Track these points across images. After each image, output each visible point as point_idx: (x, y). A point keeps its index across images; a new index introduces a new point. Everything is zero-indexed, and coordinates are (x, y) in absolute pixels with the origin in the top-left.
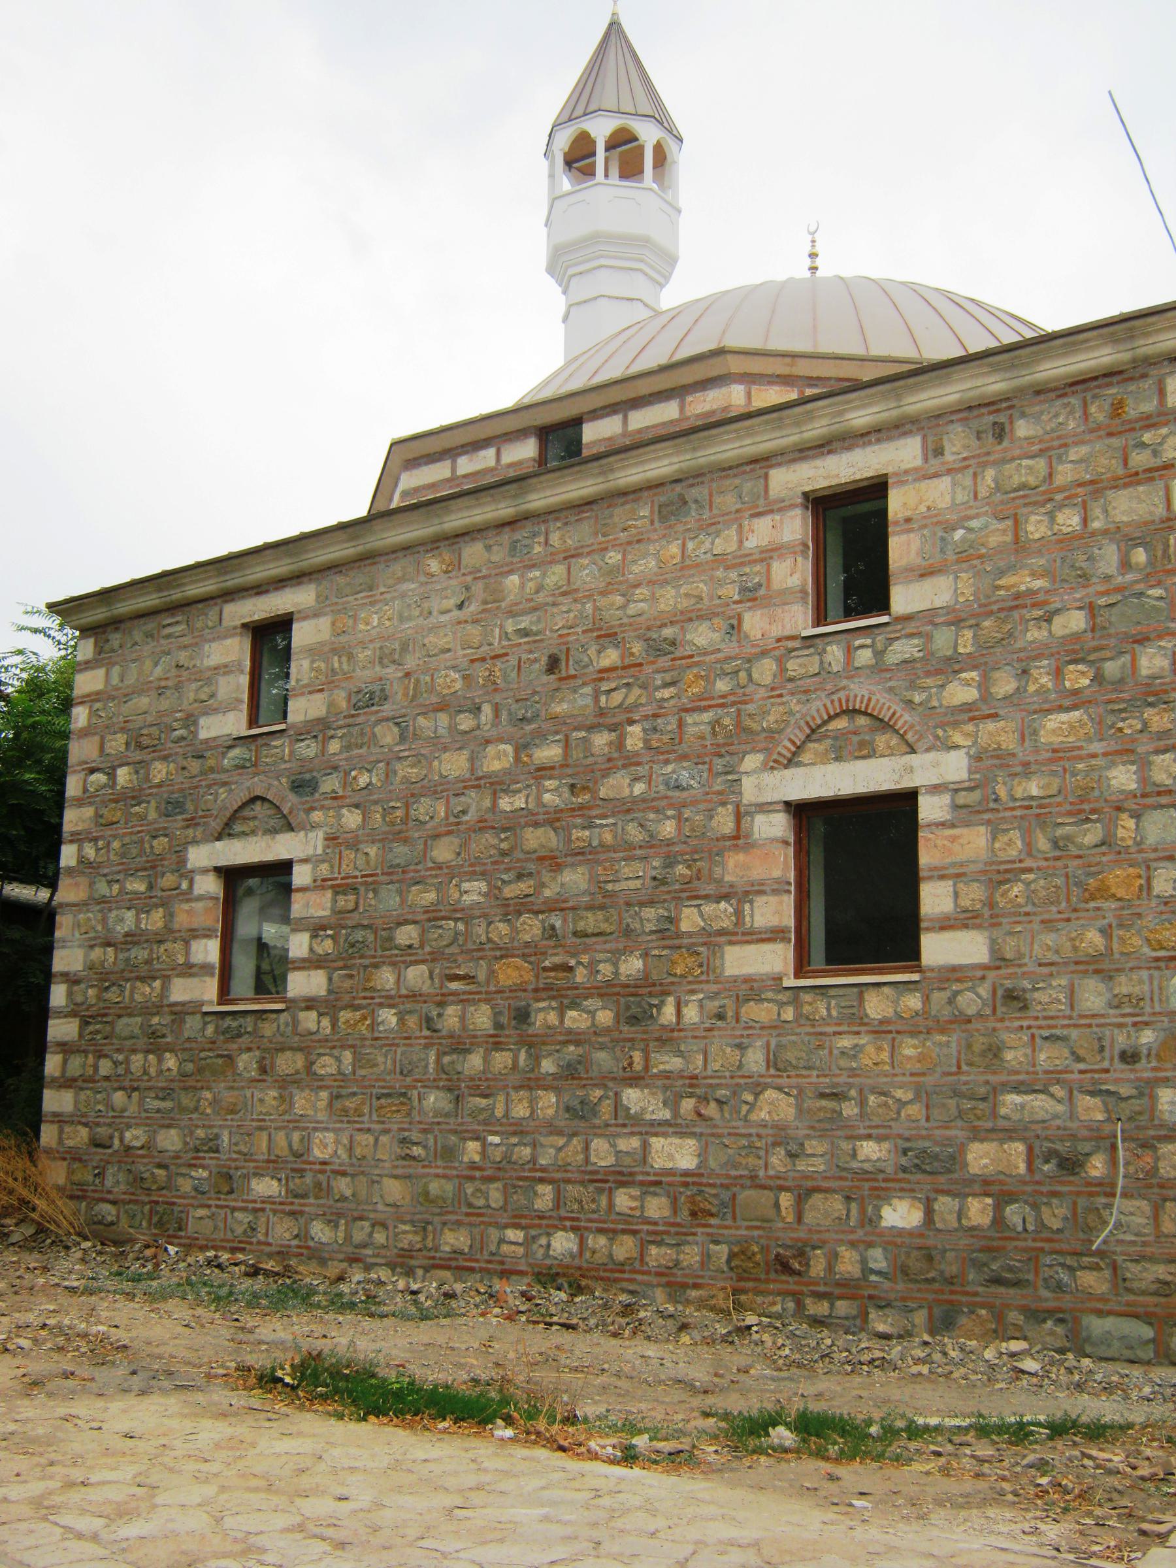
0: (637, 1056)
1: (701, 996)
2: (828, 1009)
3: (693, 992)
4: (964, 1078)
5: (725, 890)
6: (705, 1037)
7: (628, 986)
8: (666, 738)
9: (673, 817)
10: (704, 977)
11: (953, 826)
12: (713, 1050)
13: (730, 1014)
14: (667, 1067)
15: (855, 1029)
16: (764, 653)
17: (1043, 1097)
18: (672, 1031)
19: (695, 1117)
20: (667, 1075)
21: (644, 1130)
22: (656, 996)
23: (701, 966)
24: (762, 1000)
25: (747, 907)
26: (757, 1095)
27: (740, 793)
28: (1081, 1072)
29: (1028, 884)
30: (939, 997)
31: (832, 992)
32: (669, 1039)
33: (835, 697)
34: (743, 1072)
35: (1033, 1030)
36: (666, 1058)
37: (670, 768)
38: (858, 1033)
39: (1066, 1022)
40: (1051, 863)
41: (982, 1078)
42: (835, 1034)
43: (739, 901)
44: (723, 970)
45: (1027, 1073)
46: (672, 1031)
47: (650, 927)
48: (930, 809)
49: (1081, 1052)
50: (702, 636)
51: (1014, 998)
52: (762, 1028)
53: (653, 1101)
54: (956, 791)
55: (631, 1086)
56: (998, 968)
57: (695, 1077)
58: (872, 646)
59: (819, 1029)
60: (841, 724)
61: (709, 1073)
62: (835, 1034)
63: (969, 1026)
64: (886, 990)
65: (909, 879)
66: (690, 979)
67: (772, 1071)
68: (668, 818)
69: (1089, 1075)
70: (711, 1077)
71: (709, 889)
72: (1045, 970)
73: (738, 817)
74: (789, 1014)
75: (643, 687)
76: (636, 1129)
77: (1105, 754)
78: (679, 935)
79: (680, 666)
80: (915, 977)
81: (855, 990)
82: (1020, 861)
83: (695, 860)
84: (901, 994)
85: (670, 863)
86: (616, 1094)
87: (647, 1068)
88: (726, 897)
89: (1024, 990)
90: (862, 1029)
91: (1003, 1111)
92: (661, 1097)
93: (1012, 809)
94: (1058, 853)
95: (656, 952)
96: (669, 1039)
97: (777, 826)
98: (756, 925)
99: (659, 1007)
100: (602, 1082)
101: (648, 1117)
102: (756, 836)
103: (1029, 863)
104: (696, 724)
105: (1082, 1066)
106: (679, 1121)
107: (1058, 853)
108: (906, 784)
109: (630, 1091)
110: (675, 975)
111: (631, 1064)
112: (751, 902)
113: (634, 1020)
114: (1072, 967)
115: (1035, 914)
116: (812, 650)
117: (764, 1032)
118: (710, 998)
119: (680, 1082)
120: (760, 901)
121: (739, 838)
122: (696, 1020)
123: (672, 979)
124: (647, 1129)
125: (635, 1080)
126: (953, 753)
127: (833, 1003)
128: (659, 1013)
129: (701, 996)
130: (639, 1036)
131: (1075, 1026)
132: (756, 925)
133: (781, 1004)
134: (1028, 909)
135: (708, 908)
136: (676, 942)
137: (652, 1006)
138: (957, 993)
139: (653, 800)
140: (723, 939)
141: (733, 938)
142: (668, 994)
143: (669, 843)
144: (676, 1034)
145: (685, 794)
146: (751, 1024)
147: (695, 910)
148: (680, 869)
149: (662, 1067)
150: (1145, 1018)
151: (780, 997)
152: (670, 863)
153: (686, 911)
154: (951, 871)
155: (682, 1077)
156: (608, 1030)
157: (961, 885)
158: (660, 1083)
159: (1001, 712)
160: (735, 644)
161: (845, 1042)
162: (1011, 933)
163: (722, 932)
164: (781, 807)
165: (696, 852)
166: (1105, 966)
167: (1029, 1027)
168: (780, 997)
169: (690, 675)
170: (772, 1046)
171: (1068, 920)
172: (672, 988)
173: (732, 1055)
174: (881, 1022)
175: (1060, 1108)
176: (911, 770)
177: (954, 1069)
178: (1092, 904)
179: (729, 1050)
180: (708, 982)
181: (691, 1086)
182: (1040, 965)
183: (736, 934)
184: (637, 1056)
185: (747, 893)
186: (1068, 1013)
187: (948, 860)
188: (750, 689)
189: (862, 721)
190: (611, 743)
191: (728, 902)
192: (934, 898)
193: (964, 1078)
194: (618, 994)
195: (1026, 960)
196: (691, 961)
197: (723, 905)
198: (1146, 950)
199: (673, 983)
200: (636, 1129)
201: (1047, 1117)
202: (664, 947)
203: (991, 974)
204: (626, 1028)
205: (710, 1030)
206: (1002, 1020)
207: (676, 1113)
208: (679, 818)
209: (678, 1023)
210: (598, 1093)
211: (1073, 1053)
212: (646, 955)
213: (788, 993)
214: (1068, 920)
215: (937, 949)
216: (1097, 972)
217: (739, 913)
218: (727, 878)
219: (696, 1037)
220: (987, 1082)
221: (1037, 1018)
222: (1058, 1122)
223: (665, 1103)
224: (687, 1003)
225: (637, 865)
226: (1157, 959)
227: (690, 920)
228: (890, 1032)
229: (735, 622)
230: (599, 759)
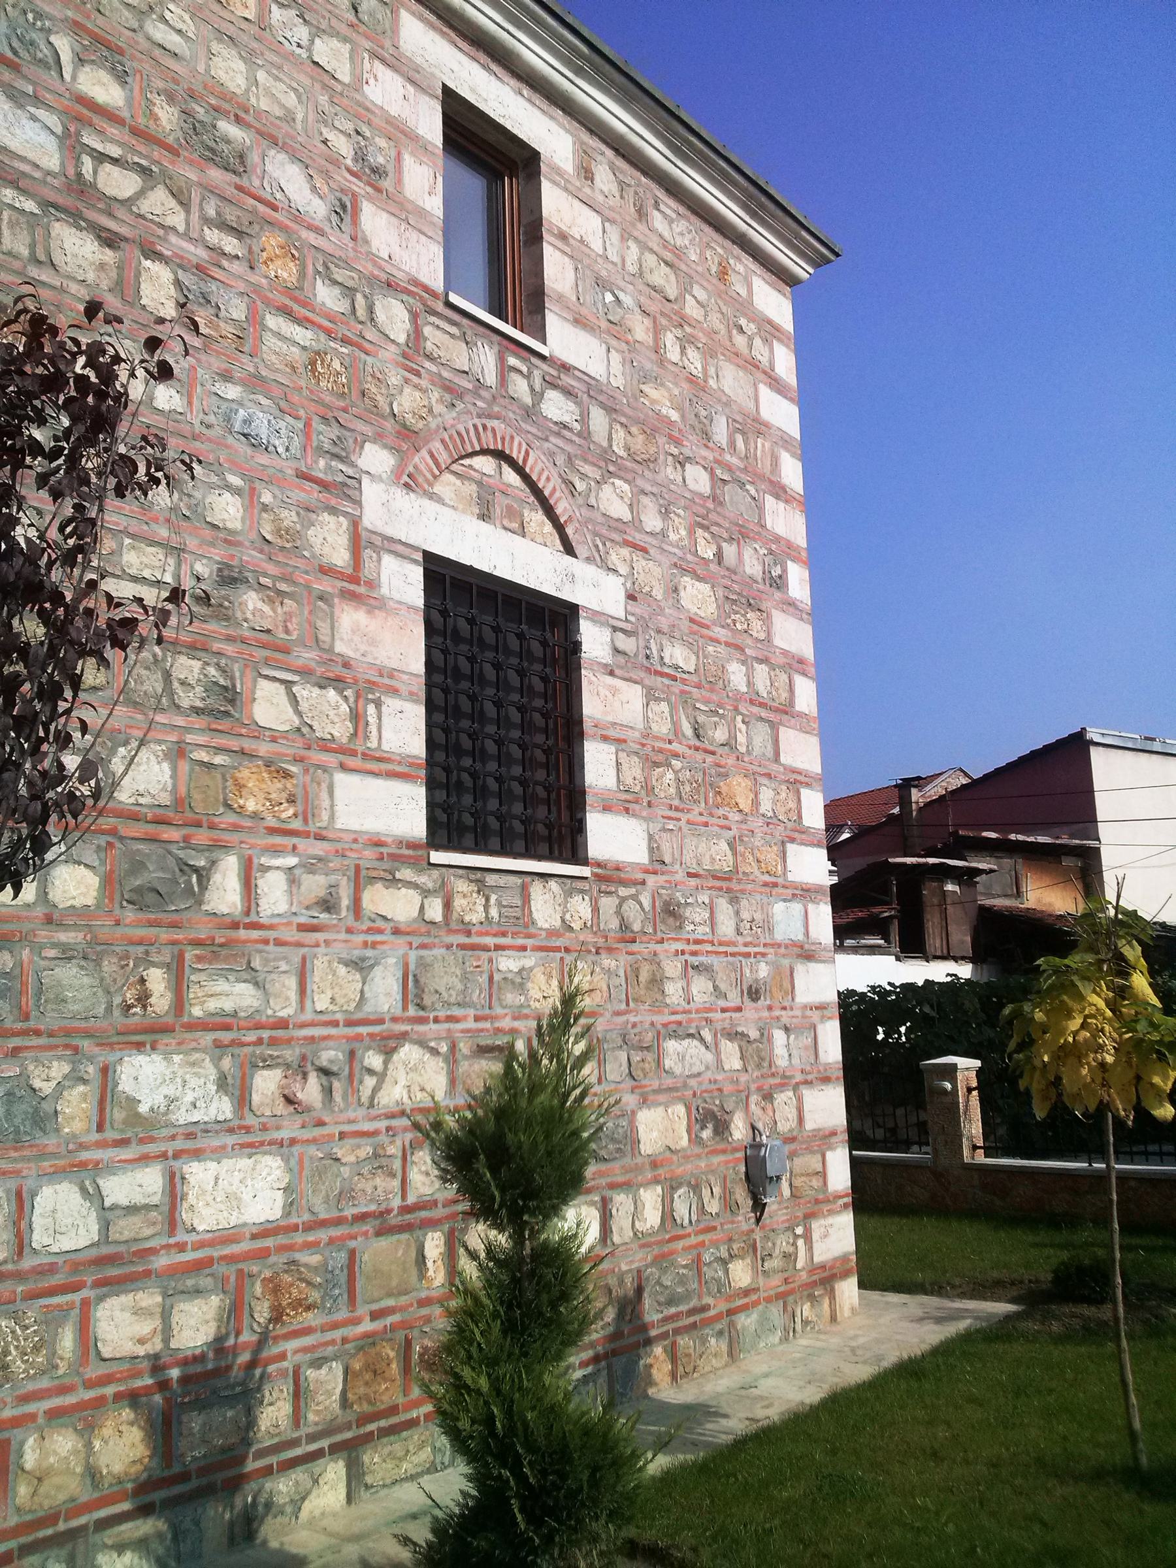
0: (157, 980)
1: (292, 861)
2: (486, 907)
3: (276, 851)
4: (632, 1018)
5: (339, 670)
6: (299, 945)
7: (134, 817)
8: (228, 329)
9: (237, 491)
10: (296, 825)
11: (611, 673)
12: (320, 965)
13: (345, 902)
14: (228, 1005)
15: (520, 941)
16: (390, 286)
17: (696, 1042)
18: (235, 926)
19: (281, 1108)
20: (222, 1023)
21: (170, 1147)
22: (198, 849)
23: (291, 801)
24: (393, 882)
25: (371, 709)
26: (388, 1053)
27: (358, 503)
28: (724, 1010)
29: (676, 772)
30: (608, 904)
31: (491, 879)
32: (233, 944)
33: (490, 423)
34: (368, 1009)
35: (687, 957)
36: (222, 986)
37: (232, 392)
38: (523, 948)
39: (709, 948)
40: (691, 752)
41: (648, 1018)
42: (498, 948)
43: (358, 696)
44: (332, 817)
45: (685, 1012)
46: (235, 926)
47: (187, 699)
48: (593, 642)
49: (723, 986)
50: (288, 179)
51: (671, 912)
52: (396, 932)
53: (193, 1082)
54: (615, 629)
55: (139, 1046)
56: (655, 873)
57: (283, 1024)
58: (528, 377)
59: (475, 940)
60: (486, 464)
61: (308, 1016)
62: (498, 948)
63: (634, 947)
64: (553, 884)
65: (568, 730)
66: (271, 822)
67: (412, 1011)
68: (228, 487)
69: (728, 1014)
70: (312, 1024)
71: (306, 656)
72: (693, 882)
73: (358, 541)
74: (435, 911)
75: (181, 197)
76: (151, 1148)
77: (727, 644)
78: (258, 732)
79: (254, 212)
80: (585, 871)
81: (518, 880)
82: (670, 742)
83: (279, 593)
84: (569, 894)
85: (230, 578)
86: (105, 1070)
87: (179, 1005)
88: (338, 683)
89: (679, 905)
90: (529, 942)
91: (668, 1063)
92: (213, 1074)
93: (662, 674)
94: (698, 744)
95: (203, 756)
96: (233, 944)
97: (406, 585)
98: (385, 747)
99: (203, 875)
100: (67, 1040)
101: (182, 1116)
102: (384, 591)
103: (675, 746)
104: (278, 335)
105: (722, 1003)
106: (250, 1120)
107: (698, 744)
108: (566, 595)
109: (141, 1059)
110: (240, 811)
111: (143, 998)
112: (378, 704)
113: (141, 898)
114: (712, 883)
115: (682, 811)
116: (454, 330)
117: (401, 940)
118: (311, 869)
119: (251, 1037)
120: (391, 704)
121: (356, 585)
122: (282, 907)
123: (231, 818)
124: (179, 1144)
125: (148, 1035)
126: (612, 577)
127: (493, 898)
128: (203, 887)
129: (292, 861)
130: (164, 935)
131: (717, 953)
132: (385, 747)
133: (426, 893)
134: (676, 802)
135: (306, 693)
136: (248, 744)
137: (185, 867)
138: (623, 900)
139: (195, 437)
140: (330, 759)
141: (351, 762)
142: (225, 848)
143: (230, 539)
144: (242, 933)
145: (263, 459)
146: (380, 923)
147: (281, 689)
148: (251, 601)
149: (212, 1005)
150: (761, 949)
151: (422, 879)
152: (230, 578)
153: (265, 689)
154: (611, 733)
155: (259, 1026)
156: (83, 912)
157: (622, 755)
158: (208, 1038)
159: (652, 551)
160: (346, 238)
161: (508, 963)
162: (664, 830)
163: (326, 745)
164: (419, 557)
165: (284, 579)
166: (734, 885)
167: (683, 952)
168: (422, 879)
169: (271, 241)
170: (412, 967)
171: (706, 824)
172: (234, 838)
173: (350, 982)
174: (552, 933)
175: (709, 1057)
176: (573, 579)
177: (623, 1006)
178: (721, 812)
179: (342, 970)
180: (307, 835)
181: (273, 1042)
182: (689, 875)
183: (353, 753)
184: (157, 980)
185: (372, 685)
186: (710, 937)
187: (610, 719)
188: (371, 334)
189: (511, 477)
190: (102, 266)
191: (340, 692)
192: (599, 766)
193: (632, 1018)
194: (113, 832)
195: (677, 867)
196: (276, 787)
197: (331, 693)
198: (757, 873)
199: (236, 828)
200: (151, 1148)
201: (703, 1068)
202: (219, 750)
203: (651, 880)
204: (130, 914)
205: (314, 929)
206: (662, 941)
207: (243, 1100)
208: (249, 495)
209: (247, 913)
210: (59, 1069)
211: (716, 988)
212: (178, 752)
213: (435, 873)
214: (706, 824)
215: (610, 836)
216: (729, 890)
217: (357, 717)
218: (339, 647)
219: (279, 943)
220: (652, 1024)
221: (688, 941)
222: (709, 1075)
223: (222, 1083)
224: (266, 869)
225: (154, 555)
226: (766, 884)
227: (269, 706)
228: (558, 949)
229: (347, 200)
230: (74, 288)
